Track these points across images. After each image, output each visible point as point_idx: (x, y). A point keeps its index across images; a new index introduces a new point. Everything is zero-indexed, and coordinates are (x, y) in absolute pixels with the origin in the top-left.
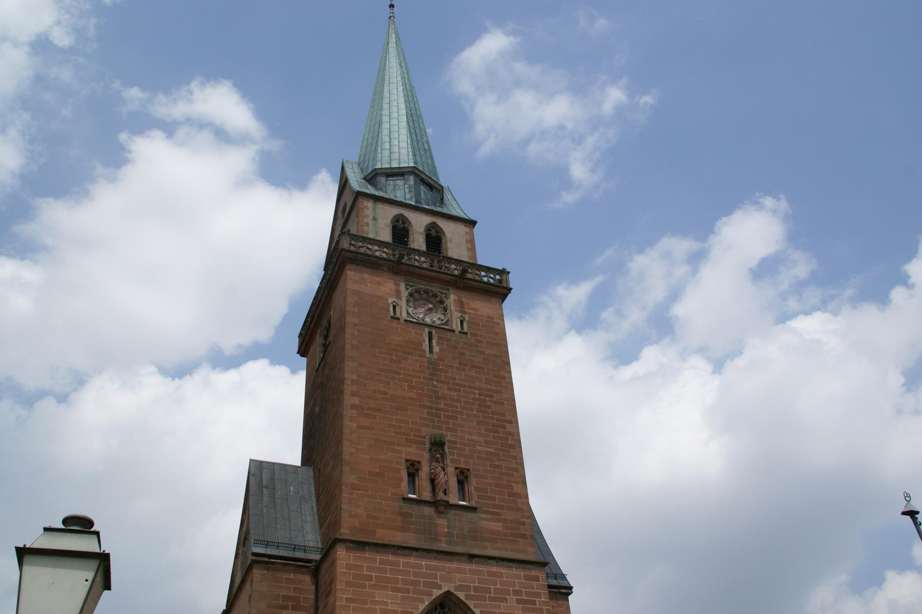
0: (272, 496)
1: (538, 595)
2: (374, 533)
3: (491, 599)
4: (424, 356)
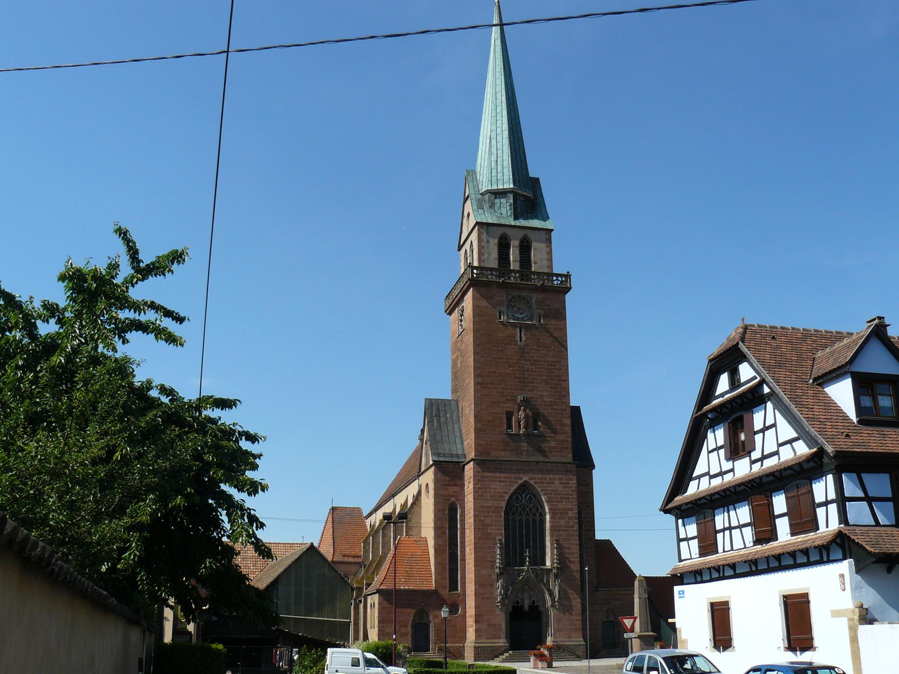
0: (439, 421)
1: (571, 480)
2: (489, 453)
3: (547, 483)
4: (516, 344)
